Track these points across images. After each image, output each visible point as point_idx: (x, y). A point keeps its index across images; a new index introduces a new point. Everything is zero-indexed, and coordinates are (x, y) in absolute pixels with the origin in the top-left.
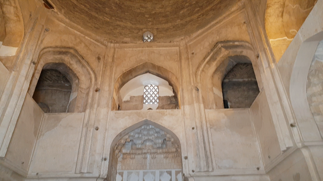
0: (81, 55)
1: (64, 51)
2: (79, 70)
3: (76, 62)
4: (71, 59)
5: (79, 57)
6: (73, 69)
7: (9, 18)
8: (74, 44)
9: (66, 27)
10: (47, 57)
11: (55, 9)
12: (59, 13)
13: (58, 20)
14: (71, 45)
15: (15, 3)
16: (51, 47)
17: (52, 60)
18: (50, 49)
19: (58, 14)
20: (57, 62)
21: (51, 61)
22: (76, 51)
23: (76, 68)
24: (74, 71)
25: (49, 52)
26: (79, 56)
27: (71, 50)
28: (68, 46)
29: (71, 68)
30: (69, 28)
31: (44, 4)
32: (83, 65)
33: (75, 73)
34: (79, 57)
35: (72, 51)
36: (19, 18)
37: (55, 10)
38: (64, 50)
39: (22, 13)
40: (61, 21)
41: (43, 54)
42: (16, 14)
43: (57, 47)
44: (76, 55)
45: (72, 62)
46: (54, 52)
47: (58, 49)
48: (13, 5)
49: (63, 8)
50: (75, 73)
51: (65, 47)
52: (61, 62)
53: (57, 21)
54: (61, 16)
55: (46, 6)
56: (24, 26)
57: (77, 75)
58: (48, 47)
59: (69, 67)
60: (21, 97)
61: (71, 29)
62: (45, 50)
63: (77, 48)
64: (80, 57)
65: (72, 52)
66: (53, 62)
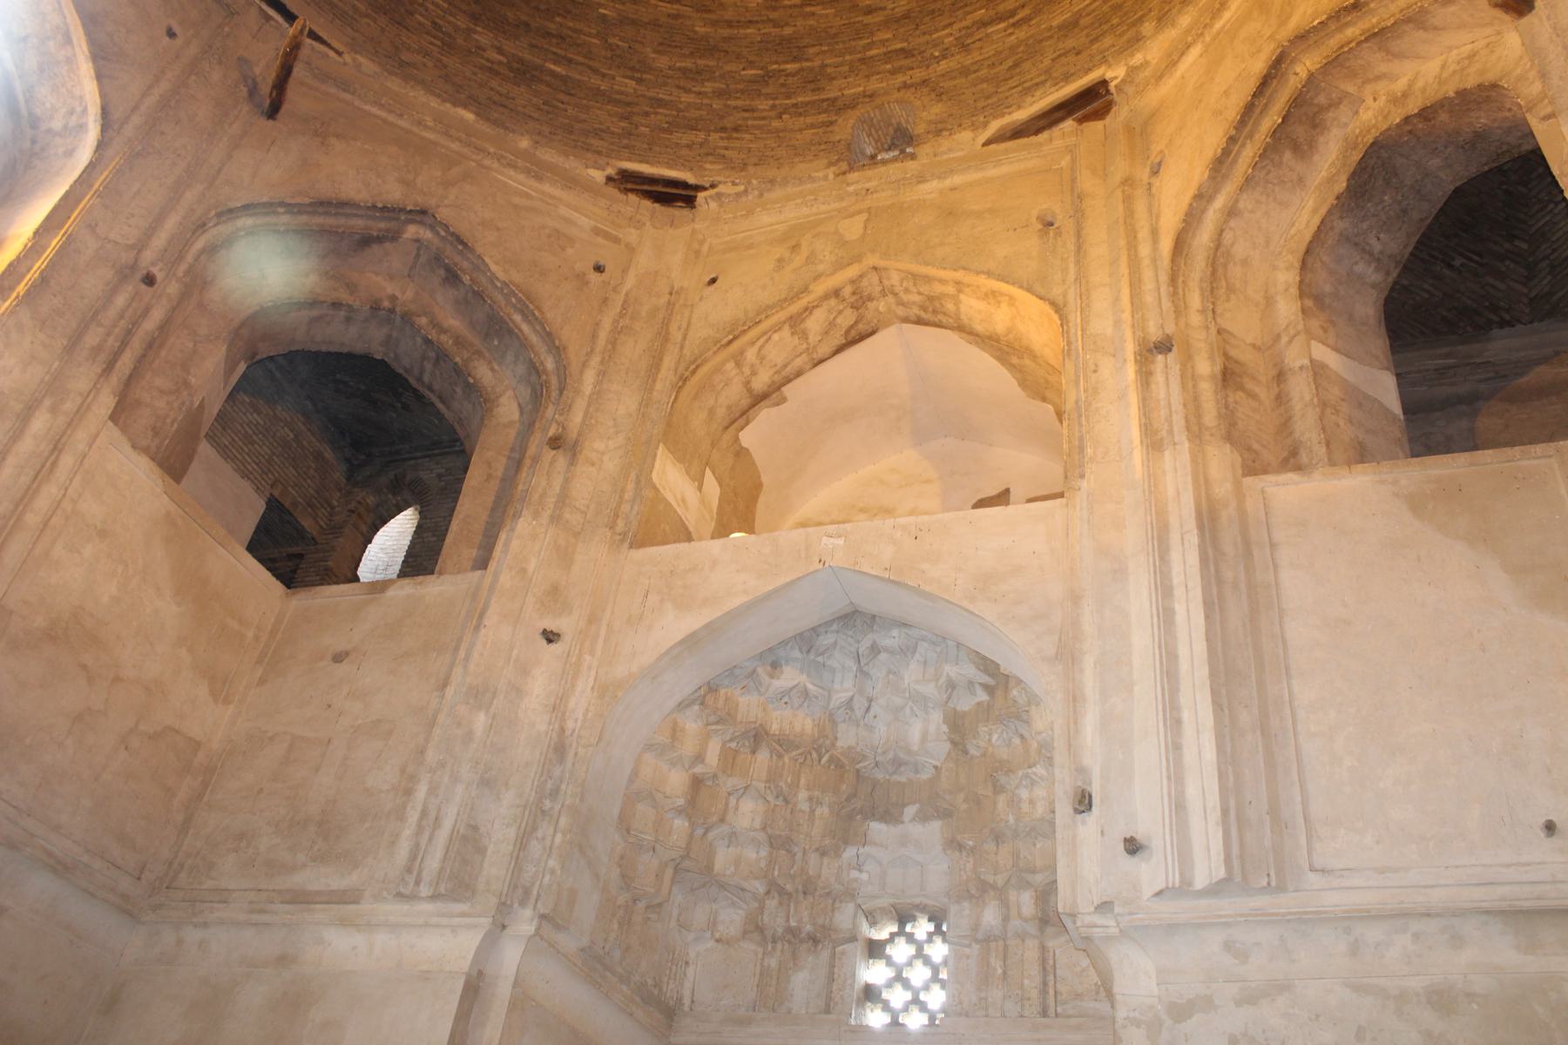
0: (1330, 18)
1: (1281, 116)
2: (1467, 49)
3: (1400, 56)
4: (1378, 78)
5: (1351, 32)
6: (1434, 94)
7: (1009, 330)
8: (1271, 37)
9: (1208, 39)
10: (1293, 231)
11: (1108, 75)
12: (1138, 58)
13: (1159, 77)
14: (1259, 66)
15: (942, 281)
16: (1202, 197)
17: (1315, 211)
18: (1220, 202)
19: (1146, 64)
20: (1341, 185)
21: (1316, 221)
22: (1303, 38)
23: (1443, 67)
24: (1440, 96)
25: (1231, 212)
26: (1340, 29)
27: (1299, 68)
28: (1251, 85)
29: (1413, 107)
30: (1218, 25)
31: (1081, 121)
32: (1409, 20)
33: (1452, 94)
34: (1351, 32)
35: (1305, 65)
36: (1002, 294)
37: (1115, 73)
38: (1271, 119)
39: (978, 273)
40: (1171, 62)
41: (1219, 256)
42: (986, 294)
43: (1221, 164)
44: (1333, 42)
45: (1400, 85)
46: (1248, 182)
47: (1248, 153)
48: (950, 289)
49: (1141, 20)
50: (1452, 94)
51: (1249, 112)
52: (1356, 156)
53: (1168, 86)
54: (1153, 51)
55: (1100, 115)
56: (1029, 290)
57: (1470, 82)
58: (1191, 219)
59: (1407, 120)
60: (1175, 537)
61: (1227, 15)
62: (1203, 238)
63: (1296, 22)
64: (1347, 25)
65: (1313, 68)
66: (1323, 211)
